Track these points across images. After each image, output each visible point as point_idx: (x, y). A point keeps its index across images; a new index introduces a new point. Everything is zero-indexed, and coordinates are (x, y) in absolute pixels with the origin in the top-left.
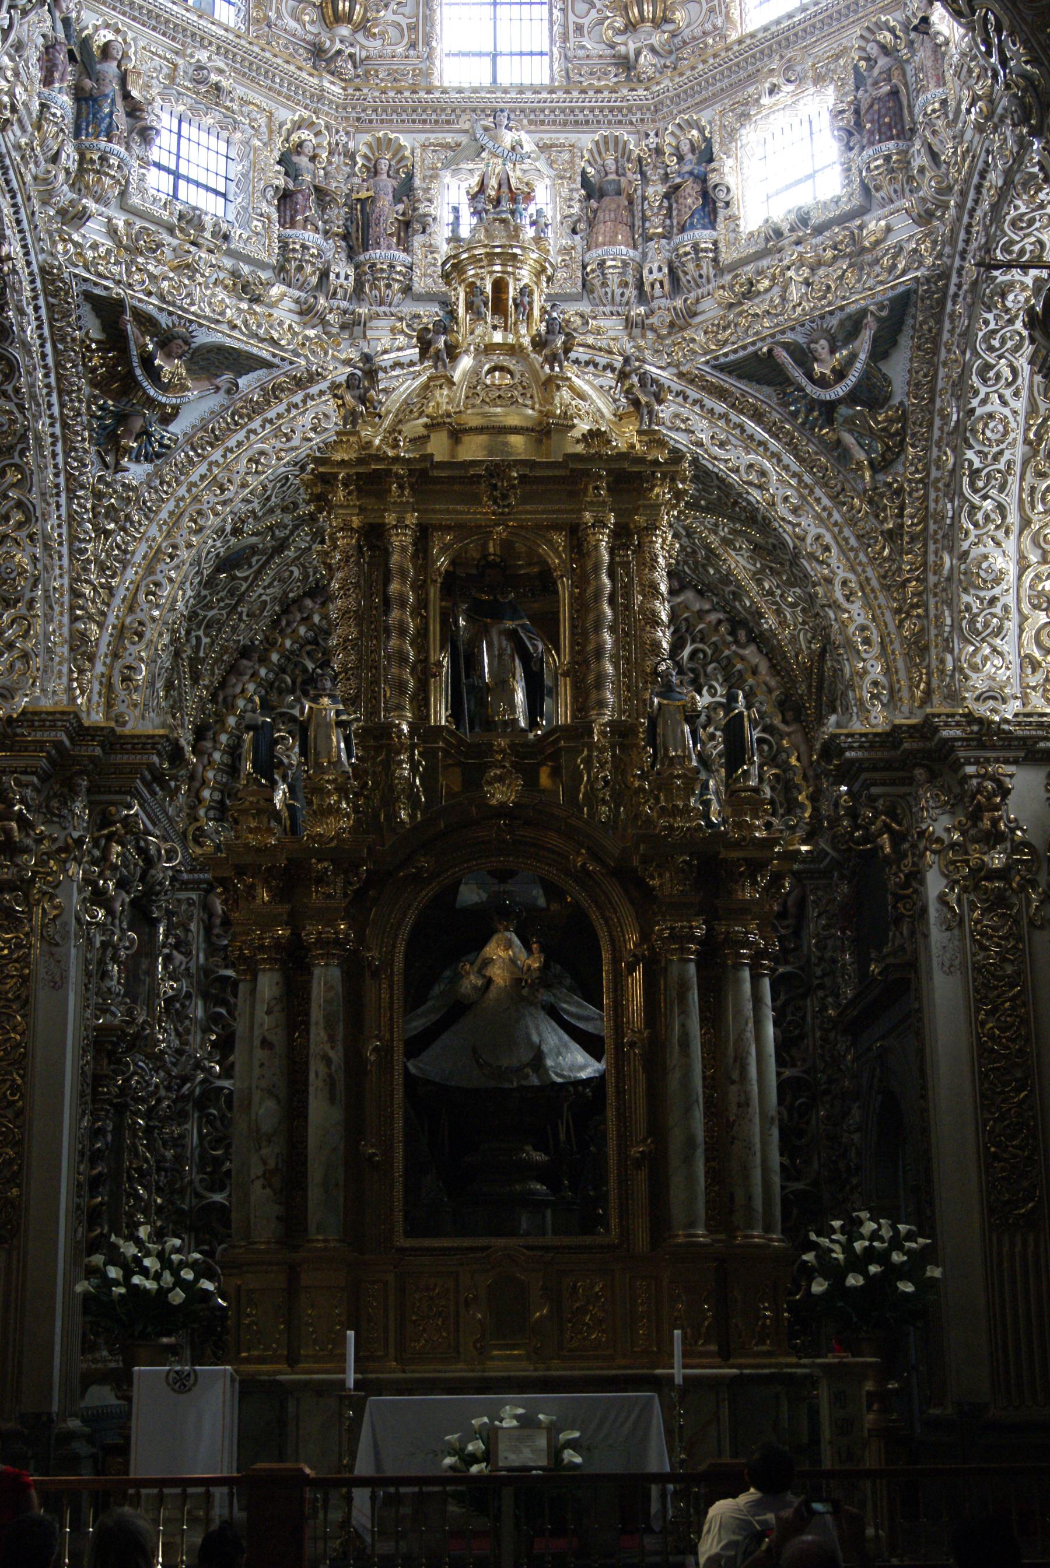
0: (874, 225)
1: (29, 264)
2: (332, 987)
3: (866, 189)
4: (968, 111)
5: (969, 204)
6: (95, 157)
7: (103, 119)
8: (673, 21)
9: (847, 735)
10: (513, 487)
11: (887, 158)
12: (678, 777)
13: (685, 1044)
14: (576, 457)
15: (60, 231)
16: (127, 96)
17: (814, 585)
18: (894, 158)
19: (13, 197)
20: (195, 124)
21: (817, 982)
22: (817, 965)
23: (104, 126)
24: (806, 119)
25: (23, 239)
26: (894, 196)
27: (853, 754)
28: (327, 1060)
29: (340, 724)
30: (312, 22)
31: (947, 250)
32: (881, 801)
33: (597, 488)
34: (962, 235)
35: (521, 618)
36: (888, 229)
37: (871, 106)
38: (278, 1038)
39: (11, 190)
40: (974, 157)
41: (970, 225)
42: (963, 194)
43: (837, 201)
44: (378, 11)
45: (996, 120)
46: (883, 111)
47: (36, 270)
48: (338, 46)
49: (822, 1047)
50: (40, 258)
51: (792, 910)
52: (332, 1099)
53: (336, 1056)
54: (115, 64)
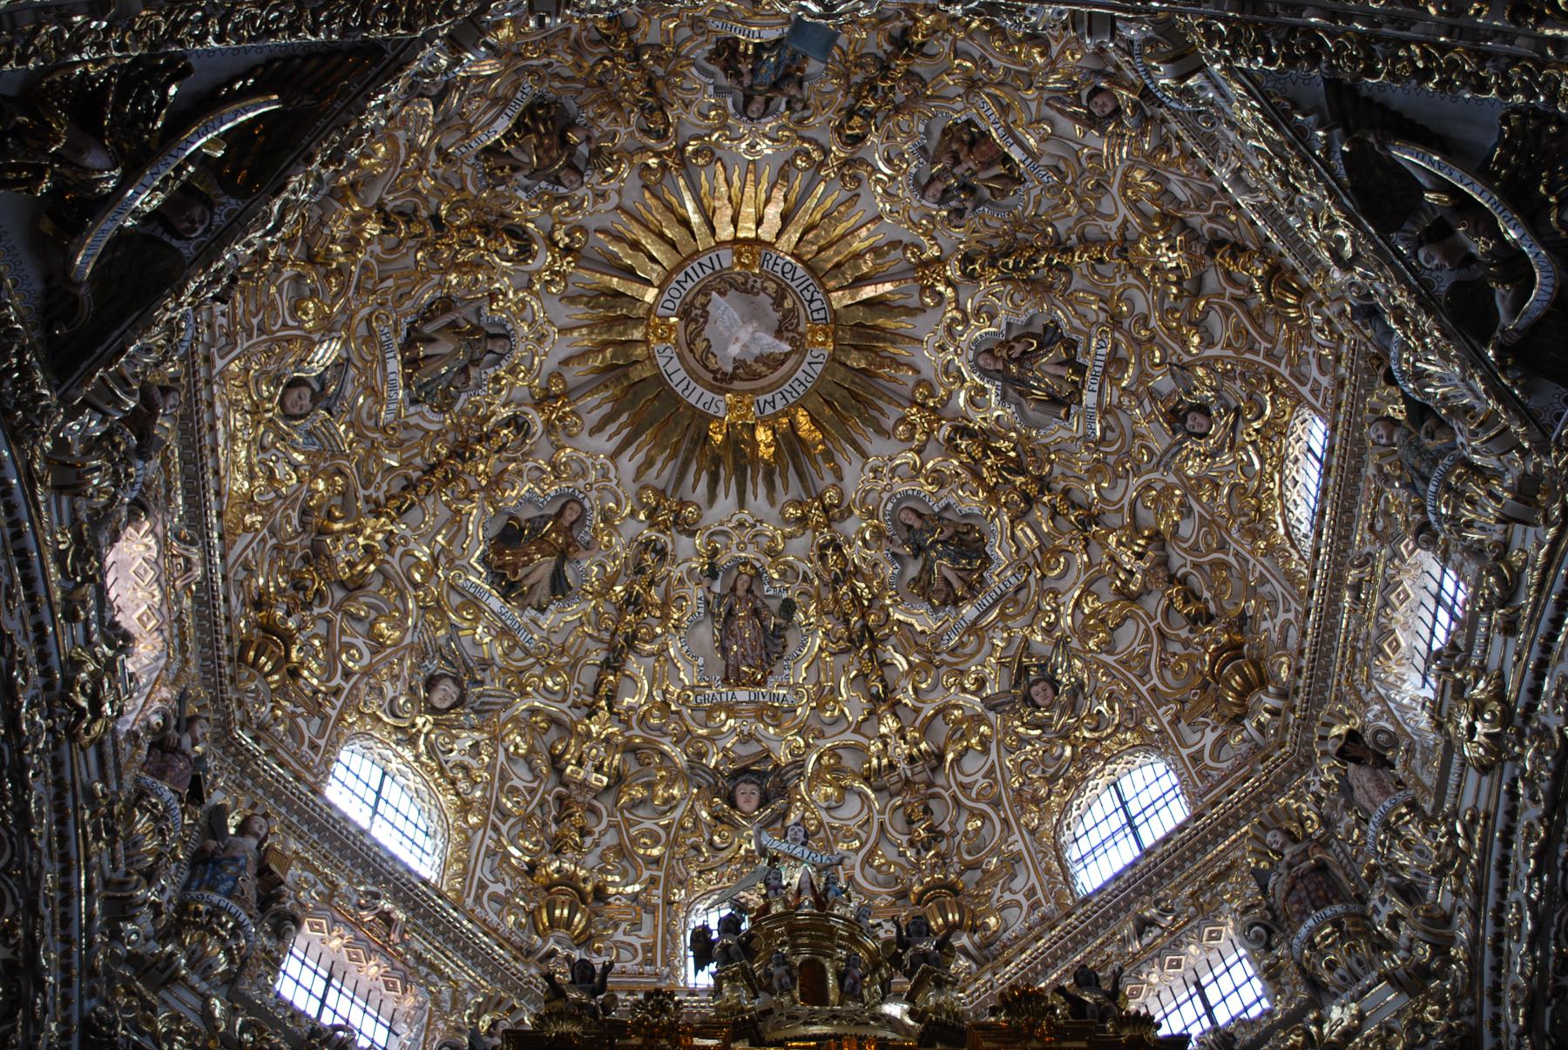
0: (1339, 1015)
1: (66, 1002)
3: (1314, 984)
4: (1471, 729)
5: (1491, 903)
6: (201, 907)
7: (223, 881)
8: (985, 926)
11: (1337, 924)
15: (127, 984)
16: (263, 871)
18: (1346, 922)
19: (66, 872)
20: (350, 982)
23: (223, 887)
24: (1190, 976)
25: (66, 954)
26: (1359, 970)
30: (518, 924)
31: (1466, 1004)
34: (1488, 959)
36: (1361, 1016)
37: (1293, 887)
39: (65, 858)
40: (1487, 817)
41: (1499, 937)
42: (1479, 890)
43: (1268, 1013)
44: (606, 928)
45: (1518, 721)
46: (1312, 887)
47: (75, 1019)
48: (551, 945)
50: (87, 1004)
54: (253, 842)
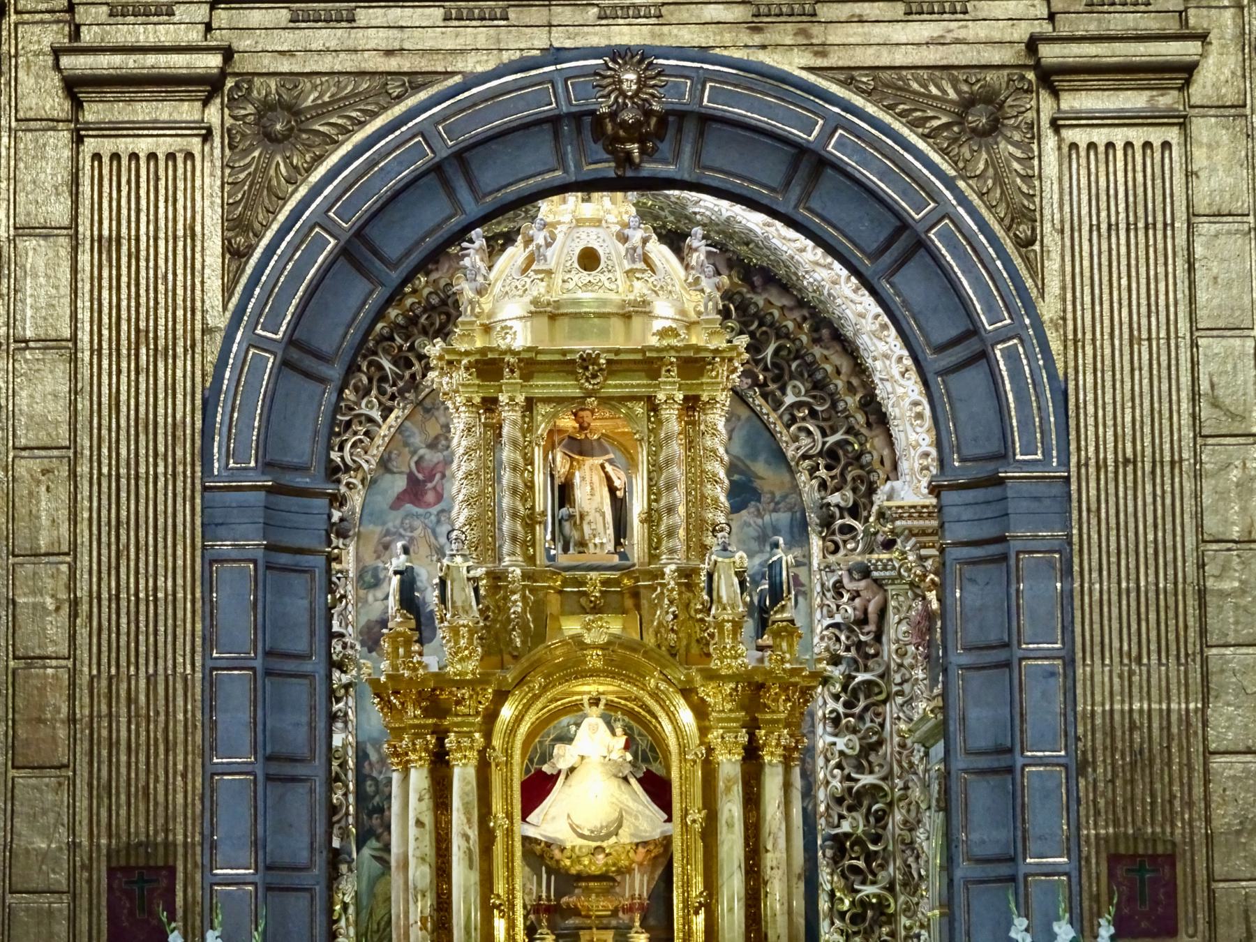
2: (468, 783)
9: (898, 507)
10: (601, 370)
12: (728, 621)
13: (730, 825)
14: (652, 349)
17: (875, 359)
21: (895, 689)
22: (896, 672)
27: (904, 523)
28: (467, 838)
29: (469, 579)
32: (930, 562)
33: (669, 371)
35: (607, 452)
38: (428, 819)
49: (900, 753)
51: (872, 616)
52: (471, 867)
53: (473, 834)
